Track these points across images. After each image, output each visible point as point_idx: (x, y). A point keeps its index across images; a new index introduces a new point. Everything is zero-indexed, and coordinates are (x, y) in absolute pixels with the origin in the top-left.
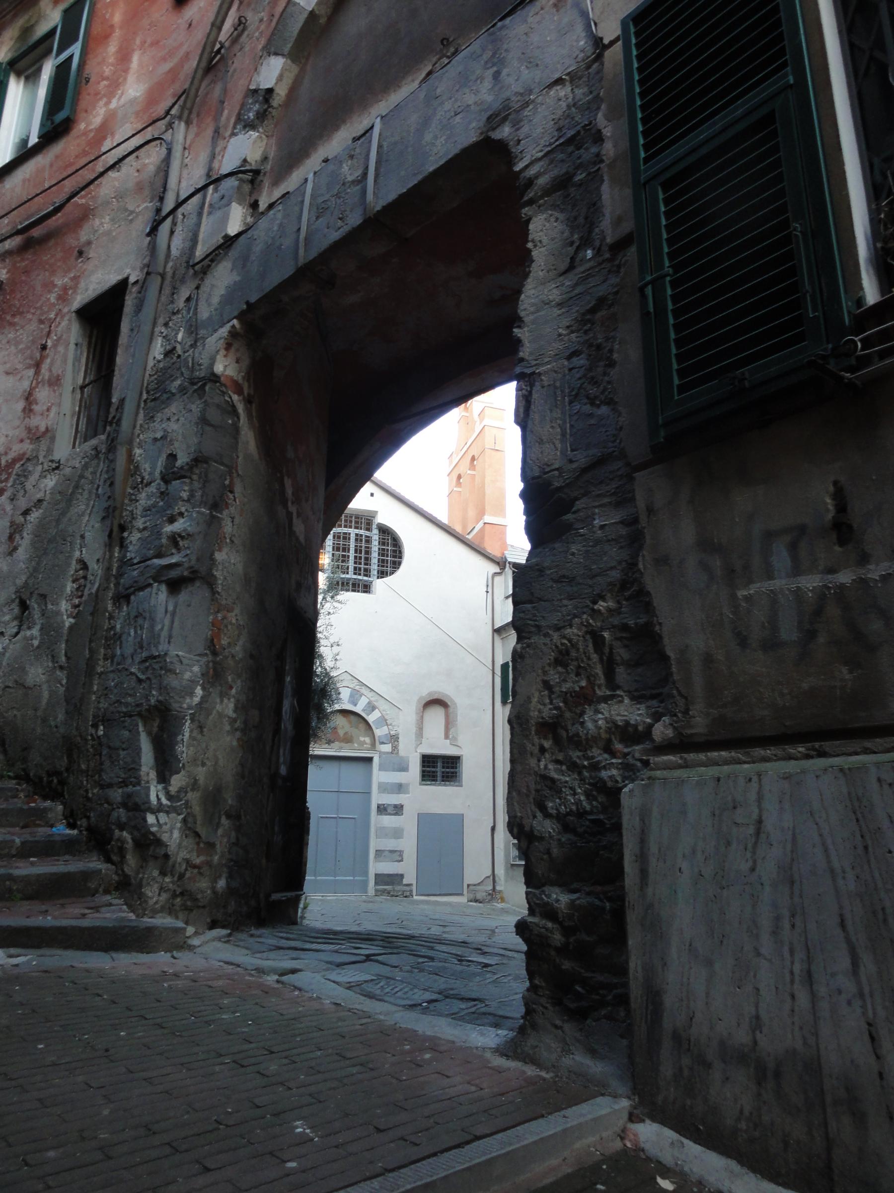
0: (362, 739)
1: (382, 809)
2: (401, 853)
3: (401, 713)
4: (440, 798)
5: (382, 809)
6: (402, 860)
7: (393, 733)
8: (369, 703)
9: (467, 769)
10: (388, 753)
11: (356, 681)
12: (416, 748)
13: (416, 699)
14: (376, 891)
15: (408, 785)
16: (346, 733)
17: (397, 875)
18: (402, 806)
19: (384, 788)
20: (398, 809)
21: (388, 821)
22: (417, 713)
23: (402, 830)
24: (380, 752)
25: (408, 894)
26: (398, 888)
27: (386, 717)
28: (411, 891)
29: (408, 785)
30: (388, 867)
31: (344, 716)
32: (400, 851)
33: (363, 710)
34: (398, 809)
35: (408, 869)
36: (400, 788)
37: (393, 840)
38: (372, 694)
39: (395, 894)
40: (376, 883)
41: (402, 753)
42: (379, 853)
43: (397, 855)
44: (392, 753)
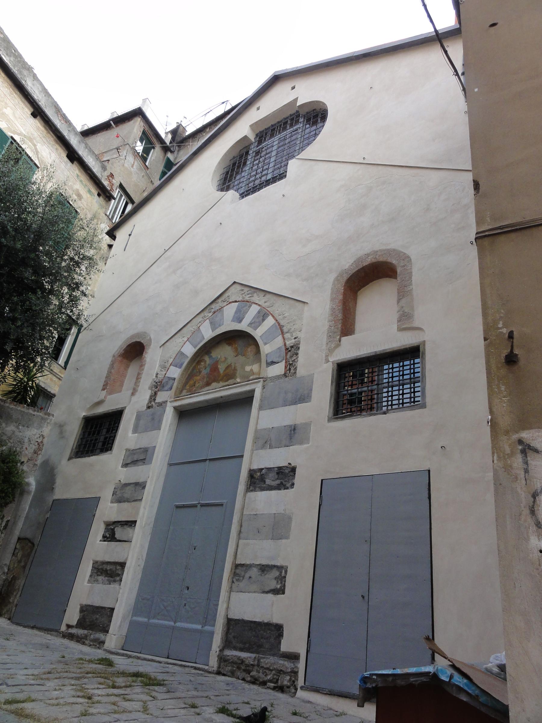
0: (248, 368)
1: (257, 480)
2: (281, 572)
3: (306, 308)
4: (375, 444)
5: (257, 480)
6: (280, 591)
7: (289, 343)
8: (259, 312)
9: (435, 369)
10: (278, 377)
11: (246, 289)
12: (327, 356)
13: (332, 277)
14: (222, 659)
15: (307, 426)
16: (229, 366)
17: (268, 626)
18: (293, 470)
19: (266, 441)
20: (285, 476)
21: (265, 501)
22: (332, 300)
23: (290, 518)
24: (265, 380)
25: (285, 680)
26: (269, 661)
27: (282, 323)
28: (295, 673)
29: (307, 426)
30: (251, 606)
31: (229, 344)
32: (279, 568)
33: (250, 324)
34: (285, 476)
35: (290, 612)
36: (293, 434)
37: (268, 544)
38: (268, 296)
39: (262, 677)
40: (227, 644)
41: (301, 371)
42: (239, 570)
43: (274, 578)
44: (285, 375)
